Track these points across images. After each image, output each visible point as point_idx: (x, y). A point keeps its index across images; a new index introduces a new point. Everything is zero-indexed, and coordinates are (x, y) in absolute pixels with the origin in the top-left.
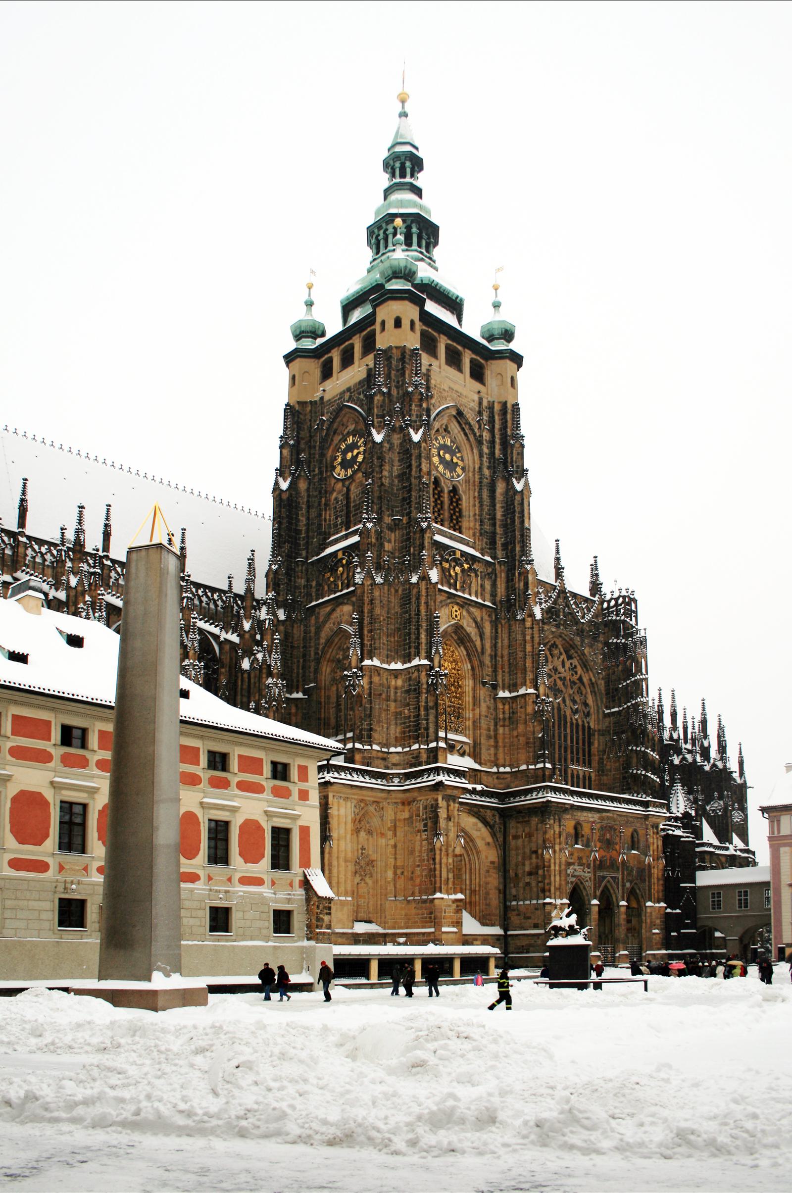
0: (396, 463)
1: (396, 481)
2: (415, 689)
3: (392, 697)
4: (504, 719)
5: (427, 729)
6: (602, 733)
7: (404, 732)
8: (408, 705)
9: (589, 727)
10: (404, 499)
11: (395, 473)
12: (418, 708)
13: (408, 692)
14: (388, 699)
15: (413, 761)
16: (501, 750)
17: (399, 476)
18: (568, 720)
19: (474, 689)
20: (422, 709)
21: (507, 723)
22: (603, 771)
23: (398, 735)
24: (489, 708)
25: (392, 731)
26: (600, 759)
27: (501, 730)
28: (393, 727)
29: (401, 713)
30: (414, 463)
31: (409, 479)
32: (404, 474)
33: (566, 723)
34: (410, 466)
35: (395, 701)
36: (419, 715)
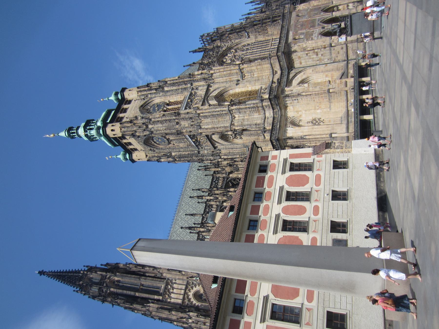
0: (158, 126)
1: (164, 125)
2: (239, 110)
3: (243, 118)
4: (251, 75)
5: (254, 104)
6: (256, 37)
7: (256, 112)
8: (245, 112)
9: (254, 43)
10: (170, 122)
11: (161, 126)
12: (246, 108)
13: (240, 112)
14: (243, 120)
15: (268, 107)
16: (263, 74)
17: (162, 124)
18: (251, 51)
19: (240, 88)
20: (246, 107)
21: (253, 74)
22: (272, 34)
23: (258, 114)
24: (247, 81)
25: (256, 116)
26: (267, 36)
27: (255, 75)
28: (255, 117)
29: (249, 114)
30: (157, 120)
31: (162, 121)
32: (161, 123)
33: (252, 52)
34: (158, 121)
35: (244, 117)
36: (249, 108)
